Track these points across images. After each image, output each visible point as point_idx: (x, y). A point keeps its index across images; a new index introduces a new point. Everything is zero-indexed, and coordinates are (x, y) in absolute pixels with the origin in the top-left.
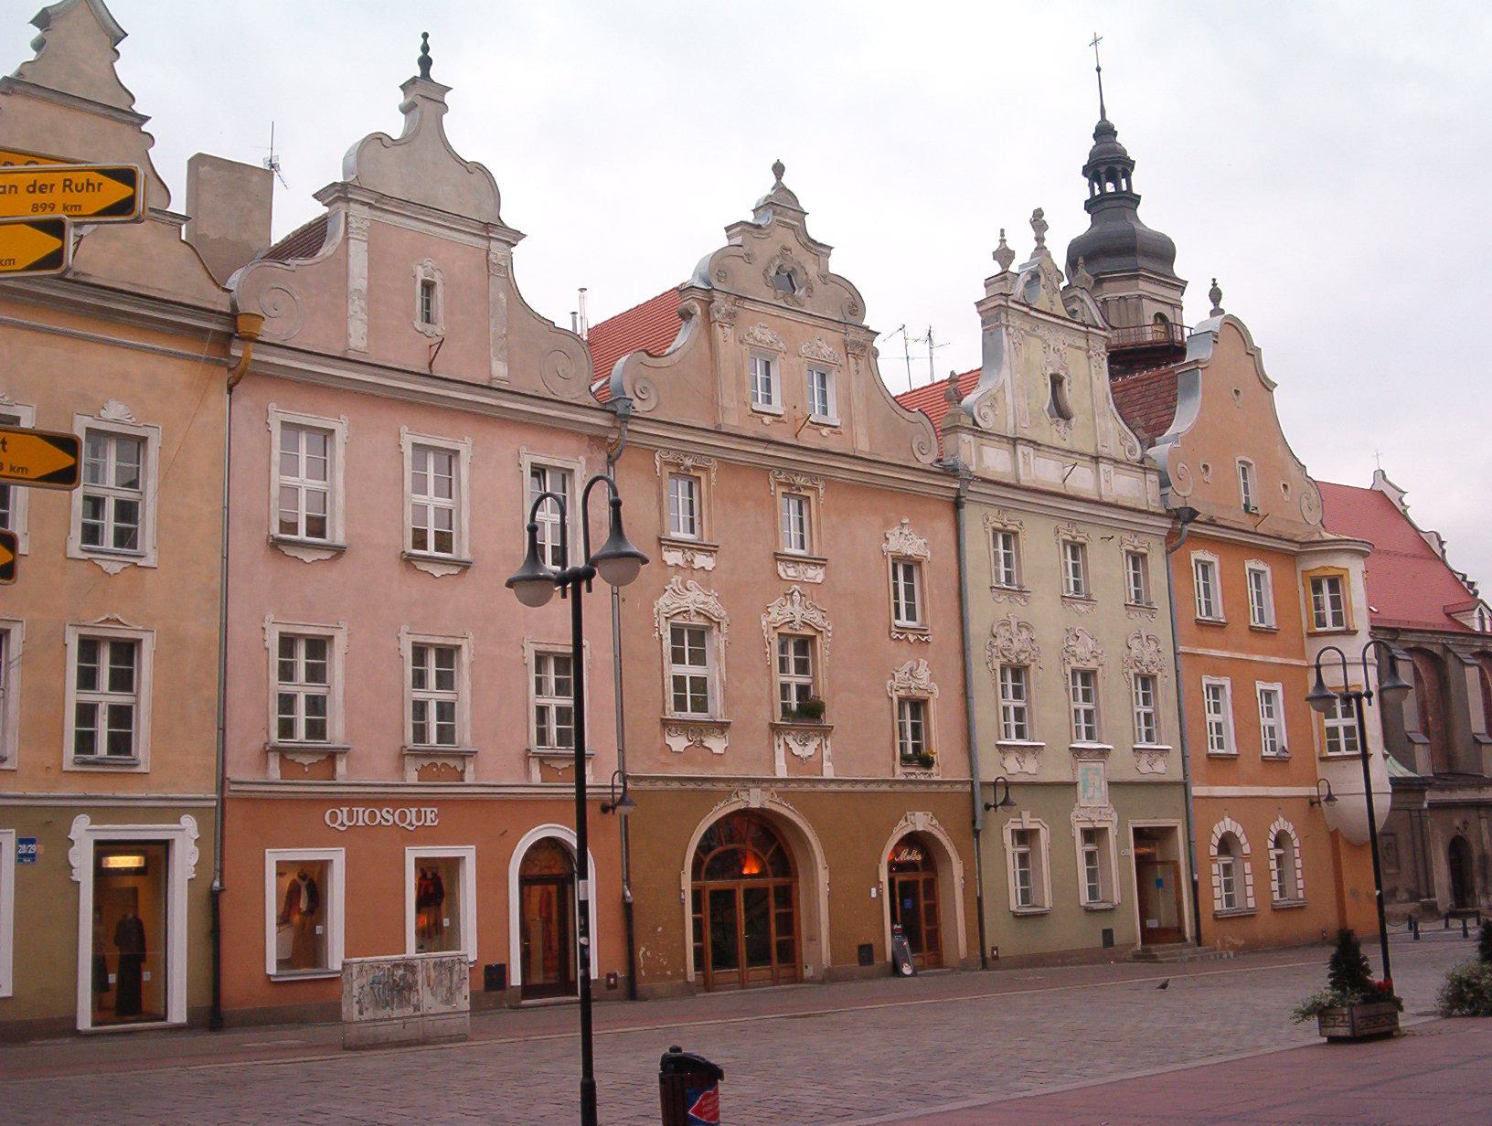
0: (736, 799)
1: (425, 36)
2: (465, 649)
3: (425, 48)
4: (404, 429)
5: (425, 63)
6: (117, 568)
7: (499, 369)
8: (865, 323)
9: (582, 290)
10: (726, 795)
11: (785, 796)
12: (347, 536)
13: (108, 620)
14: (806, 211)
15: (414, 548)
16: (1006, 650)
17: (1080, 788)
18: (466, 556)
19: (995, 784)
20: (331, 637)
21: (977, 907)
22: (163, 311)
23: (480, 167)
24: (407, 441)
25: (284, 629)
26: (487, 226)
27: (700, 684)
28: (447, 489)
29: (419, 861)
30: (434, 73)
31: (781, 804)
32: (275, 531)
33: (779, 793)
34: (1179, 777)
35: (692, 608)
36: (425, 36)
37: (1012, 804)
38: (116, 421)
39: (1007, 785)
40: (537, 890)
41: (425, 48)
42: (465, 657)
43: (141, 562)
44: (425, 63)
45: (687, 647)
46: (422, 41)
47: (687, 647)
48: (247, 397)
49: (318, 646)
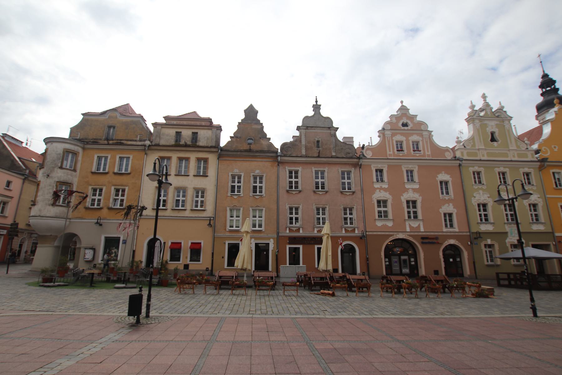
0: (395, 236)
1: (316, 97)
2: (327, 207)
3: (316, 99)
4: (313, 168)
5: (316, 102)
6: (258, 197)
7: (334, 154)
8: (428, 130)
9: (371, 138)
10: (392, 235)
11: (410, 236)
12: (301, 188)
13: (257, 206)
14: (409, 108)
15: (316, 189)
16: (479, 200)
17: (509, 234)
18: (327, 190)
19: (476, 233)
20: (299, 207)
21: (474, 264)
22: (265, 154)
23: (328, 118)
24: (314, 170)
25: (290, 206)
26: (329, 128)
27: (386, 212)
28: (322, 178)
29: (299, 248)
30: (318, 103)
31: (408, 237)
32: (288, 189)
33: (408, 235)
34: (551, 231)
35: (382, 196)
36: (316, 97)
37: (482, 238)
38: (257, 173)
39: (480, 233)
40: (346, 255)
41: (316, 99)
42: (327, 209)
43: (240, 196)
44: (316, 102)
45: (382, 204)
46: (316, 98)
47: (382, 204)
48: (281, 167)
49: (297, 209)
